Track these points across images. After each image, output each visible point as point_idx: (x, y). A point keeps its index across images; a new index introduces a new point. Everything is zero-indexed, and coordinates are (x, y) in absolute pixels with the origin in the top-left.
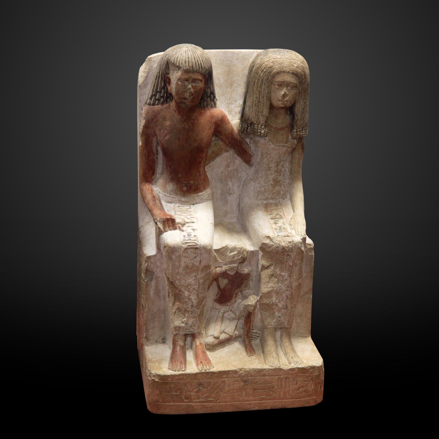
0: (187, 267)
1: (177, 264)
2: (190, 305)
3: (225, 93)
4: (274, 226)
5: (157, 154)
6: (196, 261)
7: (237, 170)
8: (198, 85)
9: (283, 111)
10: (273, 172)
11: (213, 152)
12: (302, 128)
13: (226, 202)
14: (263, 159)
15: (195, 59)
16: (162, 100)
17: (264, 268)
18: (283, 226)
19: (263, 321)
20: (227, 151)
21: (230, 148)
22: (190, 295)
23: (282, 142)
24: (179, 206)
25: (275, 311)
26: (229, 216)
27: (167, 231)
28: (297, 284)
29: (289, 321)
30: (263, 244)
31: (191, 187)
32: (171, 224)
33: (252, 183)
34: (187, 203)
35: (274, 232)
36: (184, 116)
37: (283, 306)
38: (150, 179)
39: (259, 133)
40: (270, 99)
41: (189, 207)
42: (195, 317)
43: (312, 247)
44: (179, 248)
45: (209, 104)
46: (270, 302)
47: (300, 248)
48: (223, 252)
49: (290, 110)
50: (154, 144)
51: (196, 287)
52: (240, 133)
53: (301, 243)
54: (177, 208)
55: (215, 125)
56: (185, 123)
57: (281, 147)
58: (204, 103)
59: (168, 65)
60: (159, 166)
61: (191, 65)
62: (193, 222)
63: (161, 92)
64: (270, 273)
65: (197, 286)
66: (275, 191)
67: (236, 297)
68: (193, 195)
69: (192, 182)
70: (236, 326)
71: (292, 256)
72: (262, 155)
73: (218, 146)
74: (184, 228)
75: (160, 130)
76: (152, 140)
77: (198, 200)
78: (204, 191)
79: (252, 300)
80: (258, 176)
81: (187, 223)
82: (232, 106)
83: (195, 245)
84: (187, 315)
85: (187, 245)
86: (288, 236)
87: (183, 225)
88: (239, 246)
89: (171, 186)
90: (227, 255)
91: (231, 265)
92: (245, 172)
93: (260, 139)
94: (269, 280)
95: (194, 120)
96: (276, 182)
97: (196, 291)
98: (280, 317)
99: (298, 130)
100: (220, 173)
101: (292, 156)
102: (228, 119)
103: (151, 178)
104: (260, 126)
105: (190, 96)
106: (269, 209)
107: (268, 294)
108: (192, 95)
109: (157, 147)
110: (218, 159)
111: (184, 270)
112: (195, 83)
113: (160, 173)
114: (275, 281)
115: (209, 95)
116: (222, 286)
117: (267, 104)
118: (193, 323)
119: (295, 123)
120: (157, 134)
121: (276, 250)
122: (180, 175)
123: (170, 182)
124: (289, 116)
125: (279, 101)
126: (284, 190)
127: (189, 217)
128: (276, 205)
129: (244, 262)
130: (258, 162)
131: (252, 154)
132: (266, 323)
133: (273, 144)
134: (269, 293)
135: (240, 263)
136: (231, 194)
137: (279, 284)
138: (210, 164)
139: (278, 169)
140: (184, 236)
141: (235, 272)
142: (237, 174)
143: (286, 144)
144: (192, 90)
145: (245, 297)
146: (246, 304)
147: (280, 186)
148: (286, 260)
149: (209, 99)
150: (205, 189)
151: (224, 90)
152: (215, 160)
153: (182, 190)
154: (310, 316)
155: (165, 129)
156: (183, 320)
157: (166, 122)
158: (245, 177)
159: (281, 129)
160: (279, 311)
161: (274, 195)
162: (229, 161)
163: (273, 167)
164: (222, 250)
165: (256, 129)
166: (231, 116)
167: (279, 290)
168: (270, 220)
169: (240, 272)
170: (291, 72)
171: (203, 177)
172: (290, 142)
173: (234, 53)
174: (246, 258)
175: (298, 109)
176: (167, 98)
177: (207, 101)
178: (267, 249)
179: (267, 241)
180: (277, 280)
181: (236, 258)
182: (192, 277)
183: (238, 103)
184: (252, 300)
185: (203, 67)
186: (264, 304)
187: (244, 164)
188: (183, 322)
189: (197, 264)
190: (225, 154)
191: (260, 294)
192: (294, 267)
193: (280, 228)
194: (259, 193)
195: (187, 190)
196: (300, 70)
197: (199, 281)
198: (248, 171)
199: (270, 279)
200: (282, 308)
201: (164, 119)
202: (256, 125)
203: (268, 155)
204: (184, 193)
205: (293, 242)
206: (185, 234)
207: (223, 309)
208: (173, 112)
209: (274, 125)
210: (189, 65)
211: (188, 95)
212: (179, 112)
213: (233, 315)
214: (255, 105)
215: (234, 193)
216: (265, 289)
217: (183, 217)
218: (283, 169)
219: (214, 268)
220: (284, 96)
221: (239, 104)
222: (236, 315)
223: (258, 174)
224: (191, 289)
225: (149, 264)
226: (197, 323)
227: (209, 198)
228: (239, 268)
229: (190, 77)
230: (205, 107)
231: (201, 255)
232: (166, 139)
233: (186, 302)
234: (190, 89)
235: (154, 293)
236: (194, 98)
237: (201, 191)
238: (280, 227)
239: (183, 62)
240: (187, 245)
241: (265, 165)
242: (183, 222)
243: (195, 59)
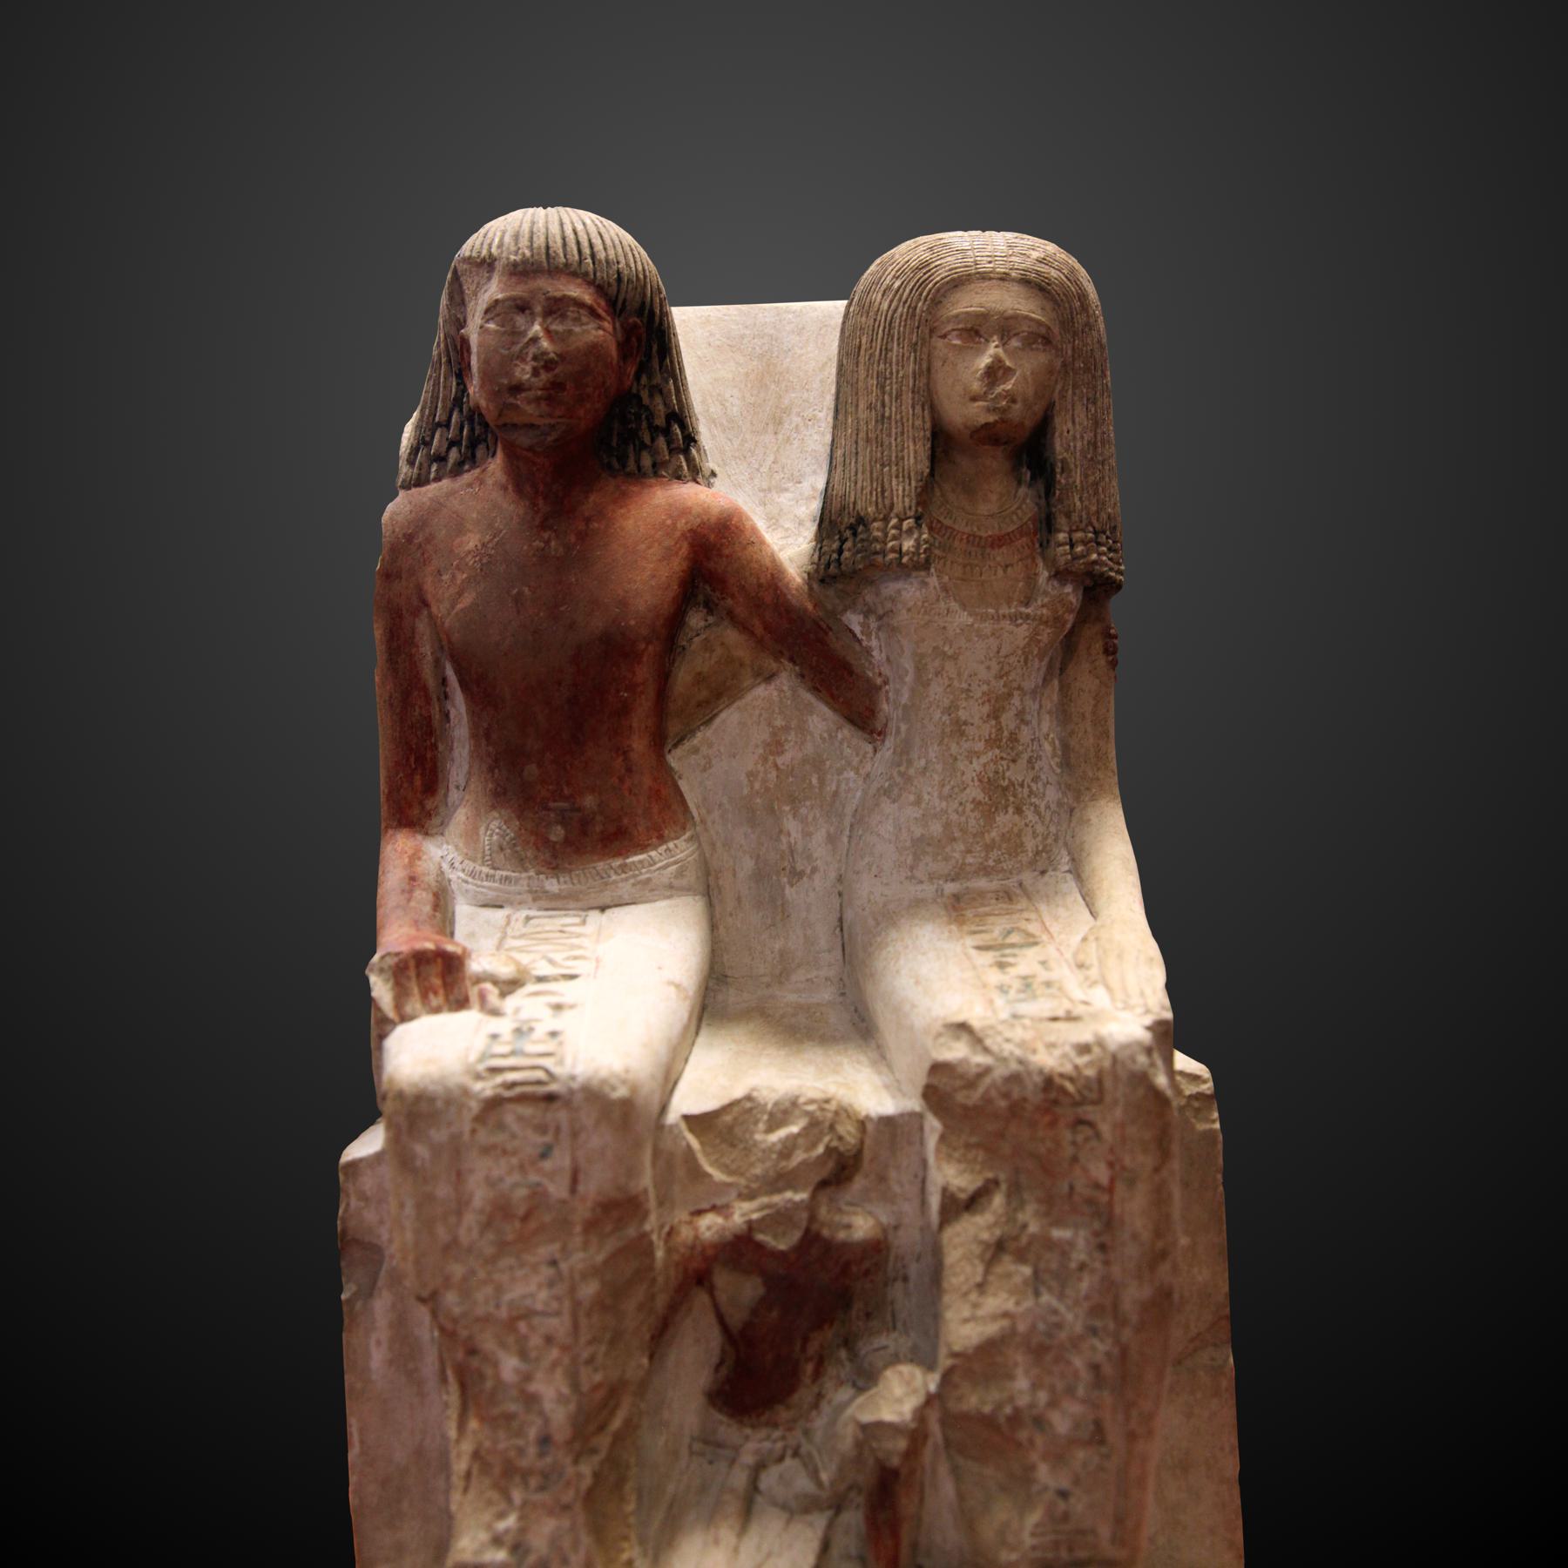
0: (501, 1210)
1: (443, 1190)
2: (532, 1433)
3: (752, 452)
4: (994, 977)
5: (446, 697)
6: (551, 1175)
7: (817, 764)
8: (577, 329)
9: (995, 461)
10: (980, 746)
11: (700, 679)
12: (1095, 532)
13: (778, 911)
14: (927, 684)
15: (562, 224)
16: (454, 455)
17: (957, 1206)
18: (1044, 976)
19: (968, 1522)
20: (770, 678)
21: (777, 656)
22: (527, 1378)
23: (1009, 602)
24: (528, 919)
25: (1034, 1457)
26: (799, 976)
27: (411, 1018)
28: (1146, 1292)
29: (1119, 1521)
30: (937, 1068)
31: (585, 825)
32: (437, 982)
33: (888, 807)
34: (572, 904)
35: (991, 1002)
36: (541, 502)
37: (1077, 1426)
38: (416, 811)
39: (892, 556)
40: (930, 403)
41: (577, 920)
42: (566, 1508)
43: (1208, 1087)
44: (449, 1101)
45: (664, 464)
46: (999, 1406)
47: (1142, 1079)
48: (730, 1128)
49: (1029, 449)
50: (426, 649)
51: (559, 1325)
52: (815, 586)
53: (1149, 1051)
54: (520, 924)
55: (692, 545)
56: (546, 535)
57: (1006, 624)
58: (638, 462)
59: (461, 286)
60: (456, 753)
61: (540, 241)
62: (573, 977)
63: (447, 425)
64: (985, 1236)
65: (567, 1318)
66: (994, 834)
67: (818, 1374)
68: (600, 865)
69: (589, 801)
70: (825, 1547)
71: (1105, 1129)
72: (920, 669)
73: (719, 651)
74: (510, 1003)
75: (439, 573)
76: (413, 630)
77: (625, 889)
78: (655, 848)
79: (898, 1396)
80: (912, 772)
81: (541, 979)
82: (784, 499)
83: (539, 1083)
84: (517, 1496)
85: (499, 1079)
86: (1070, 1018)
87: (510, 986)
88: (812, 1094)
89: (495, 829)
90: (755, 1144)
91: (776, 1199)
92: (855, 767)
93: (899, 585)
94: (987, 1272)
95: (588, 520)
96: (998, 795)
97: (565, 1348)
98: (1063, 1494)
99: (1079, 535)
100: (743, 777)
101: (1064, 689)
102: (754, 529)
103: (421, 804)
104: (894, 521)
105: (535, 372)
106: (969, 913)
107: (985, 1361)
108: (549, 365)
109: (437, 663)
110: (730, 718)
111: (487, 1225)
112: (563, 317)
113: (462, 783)
114: (1017, 1279)
115: (660, 421)
116: (736, 1319)
117: (918, 422)
118: (554, 1542)
119: (1060, 500)
120: (429, 597)
121: (1006, 1095)
122: (532, 771)
123: (493, 807)
124: (1030, 486)
125: (974, 399)
126: (1040, 829)
127: (558, 957)
128: (1007, 896)
129: (849, 1179)
130: (905, 706)
131: (879, 681)
132: (988, 1531)
133: (964, 606)
134: (989, 1349)
135: (824, 1184)
136: (801, 874)
137: (1046, 1298)
138: (695, 741)
139: (1000, 730)
140: (494, 1037)
141: (796, 1236)
142: (822, 781)
143: (1027, 605)
144: (545, 344)
145: (866, 1378)
146: (867, 1417)
147: (1019, 811)
148: (1069, 1151)
149: (661, 442)
150: (662, 839)
151: (744, 441)
152: (717, 721)
153: (547, 841)
154: (1231, 1465)
155: (458, 568)
156: (501, 1526)
157: (465, 538)
158: (859, 794)
159: (999, 541)
160: (1058, 1458)
161: (994, 854)
162: (779, 722)
163: (976, 721)
164: (728, 1118)
165: (876, 540)
166: (780, 533)
167: (1050, 1335)
168: (973, 952)
169: (825, 1233)
170: (1013, 274)
171: (647, 781)
172: (1046, 593)
173: (788, 311)
174: (858, 1155)
175: (1068, 439)
176: (473, 445)
177: (654, 452)
178: (960, 1097)
179: (956, 1051)
180: (1027, 1270)
181: (799, 1156)
182: (535, 1268)
183: (806, 485)
184: (898, 1396)
185: (601, 255)
186: (965, 1417)
187: (846, 731)
188: (497, 1541)
189: (557, 1189)
190: (761, 693)
191: (945, 1362)
192: (1120, 1188)
193: (1028, 986)
194: (920, 846)
195: (567, 841)
196: (1054, 273)
197: (572, 1290)
198: (868, 767)
199: (989, 1264)
200: (1073, 1442)
201: (459, 528)
202: (876, 525)
203: (949, 666)
204: (555, 856)
205: (1100, 1043)
206: (504, 1026)
207: (753, 1443)
208: (497, 495)
209: (961, 526)
210: (531, 247)
211: (528, 368)
212: (519, 490)
213: (803, 1484)
214: (868, 440)
215: (814, 870)
216: (966, 1324)
217: (524, 959)
218: (1025, 734)
219: (684, 1216)
220: (994, 373)
221: (814, 488)
222: (819, 1484)
223: (910, 762)
224: (535, 1341)
225: (354, 1202)
226: (576, 1544)
227: (684, 882)
228: (823, 1212)
229: (533, 293)
230: (645, 475)
231: (575, 1135)
232: (459, 606)
233: (509, 1417)
234: (535, 340)
235: (391, 1362)
236: (556, 386)
237: (643, 848)
238: (1027, 983)
239: (507, 239)
240: (499, 1079)
241: (937, 715)
242: (505, 971)
243: (562, 224)
